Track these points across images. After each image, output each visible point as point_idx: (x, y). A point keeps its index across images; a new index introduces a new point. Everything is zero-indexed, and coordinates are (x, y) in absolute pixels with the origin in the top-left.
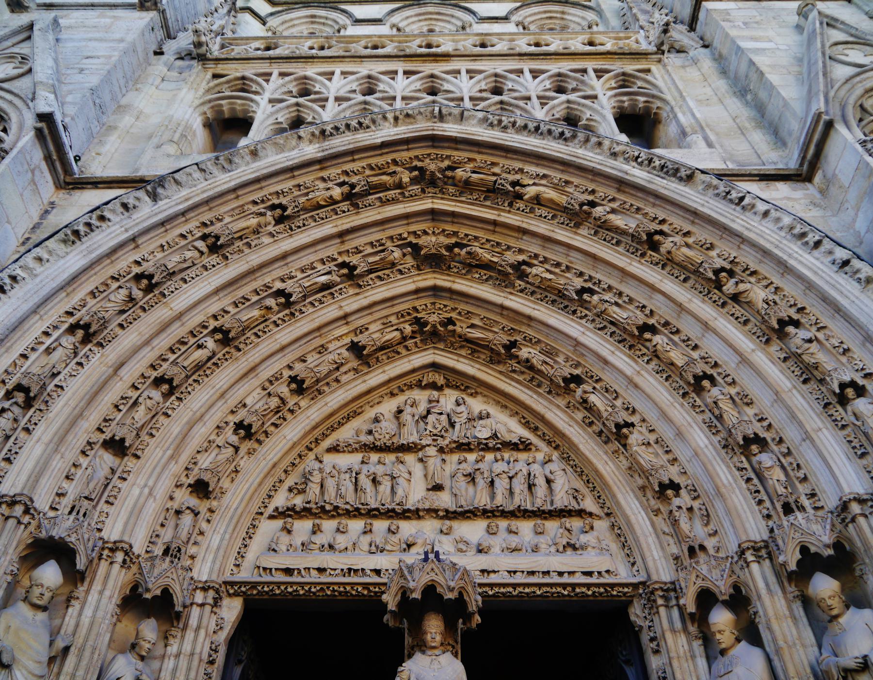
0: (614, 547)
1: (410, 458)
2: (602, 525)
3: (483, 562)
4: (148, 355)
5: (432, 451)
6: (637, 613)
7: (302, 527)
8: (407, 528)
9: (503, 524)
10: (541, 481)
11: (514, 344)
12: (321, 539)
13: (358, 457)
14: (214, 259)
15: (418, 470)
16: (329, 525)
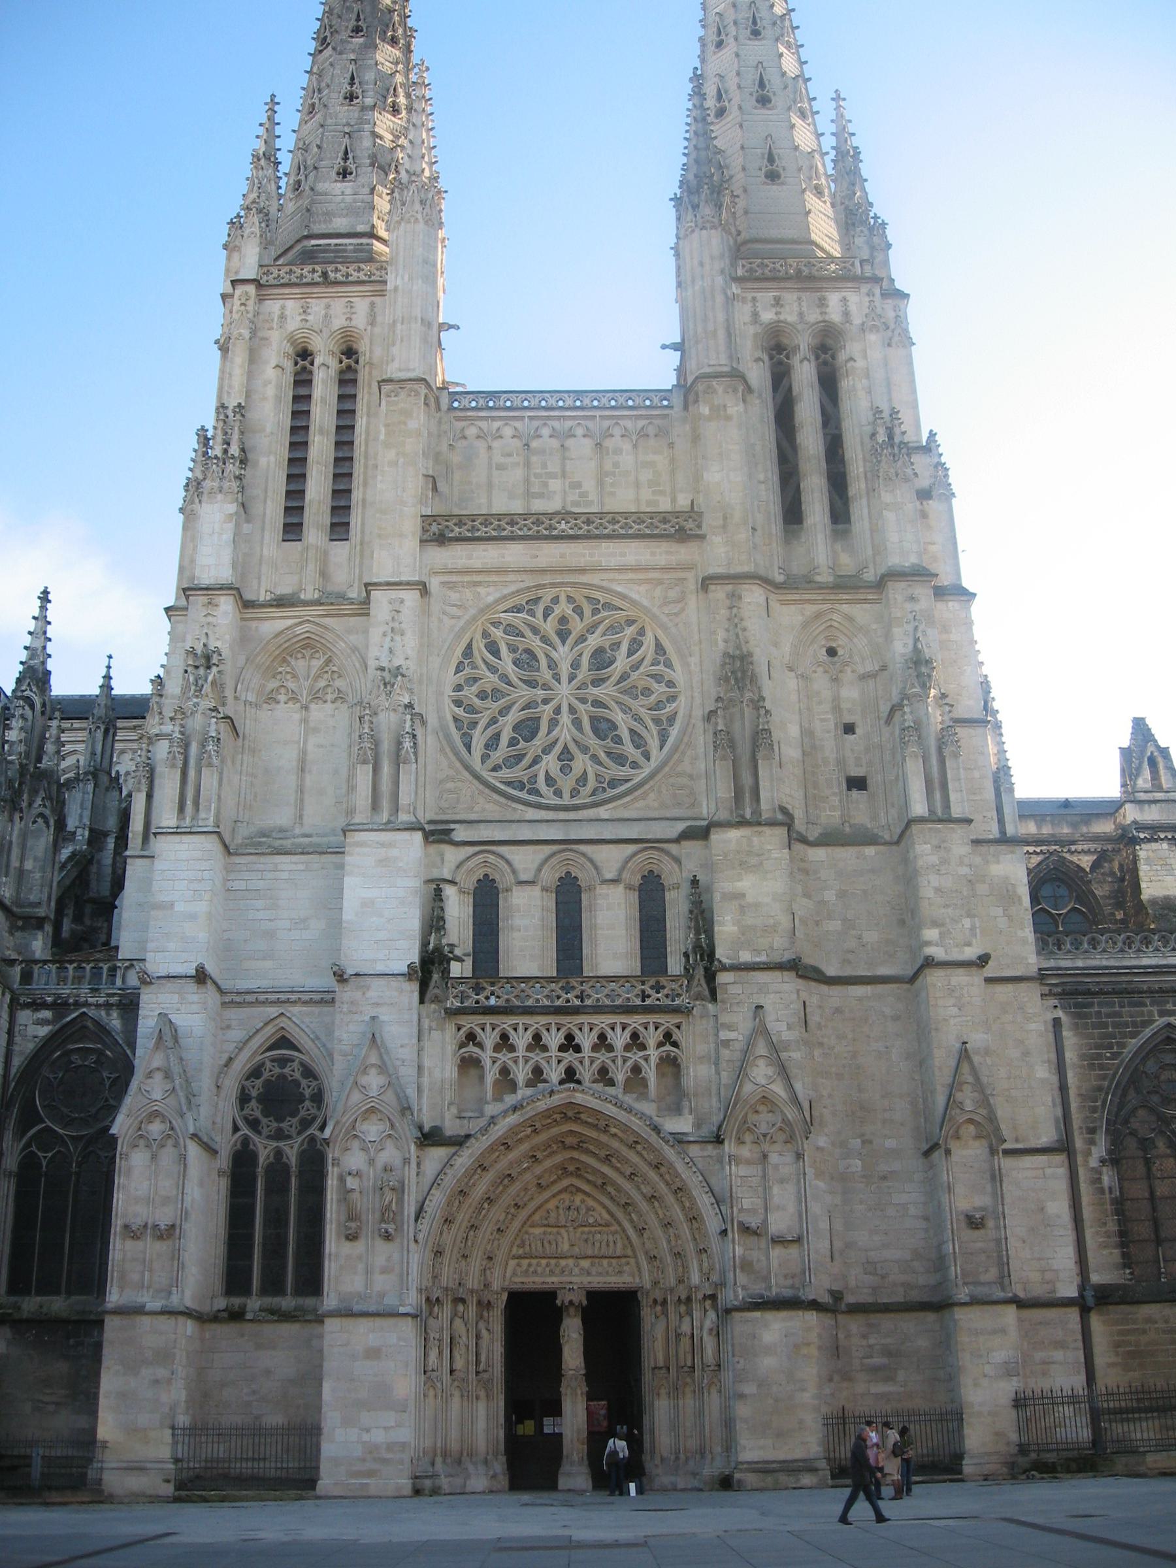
0: (636, 1270)
1: (563, 1231)
2: (632, 1261)
3: (589, 1279)
4: (467, 1216)
5: (571, 1229)
6: (639, 1294)
7: (525, 1262)
8: (563, 1262)
9: (597, 1260)
10: (611, 1244)
11: (604, 1184)
12: (532, 1269)
13: (541, 1230)
14: (484, 1173)
15: (565, 1235)
16: (534, 1261)
